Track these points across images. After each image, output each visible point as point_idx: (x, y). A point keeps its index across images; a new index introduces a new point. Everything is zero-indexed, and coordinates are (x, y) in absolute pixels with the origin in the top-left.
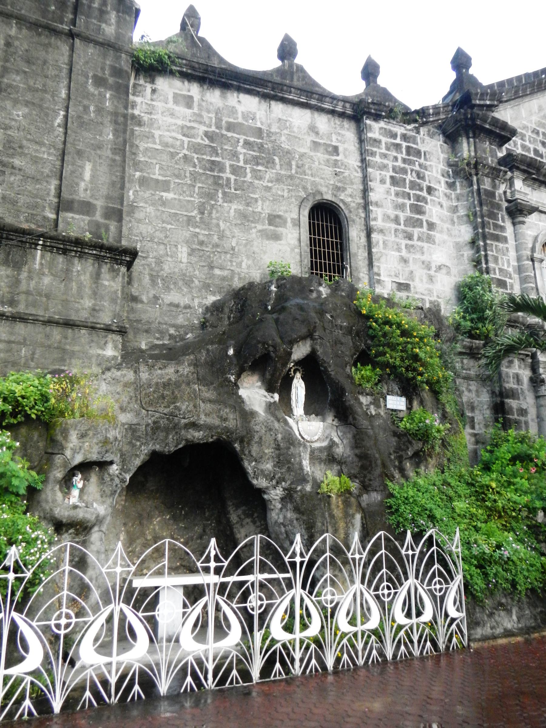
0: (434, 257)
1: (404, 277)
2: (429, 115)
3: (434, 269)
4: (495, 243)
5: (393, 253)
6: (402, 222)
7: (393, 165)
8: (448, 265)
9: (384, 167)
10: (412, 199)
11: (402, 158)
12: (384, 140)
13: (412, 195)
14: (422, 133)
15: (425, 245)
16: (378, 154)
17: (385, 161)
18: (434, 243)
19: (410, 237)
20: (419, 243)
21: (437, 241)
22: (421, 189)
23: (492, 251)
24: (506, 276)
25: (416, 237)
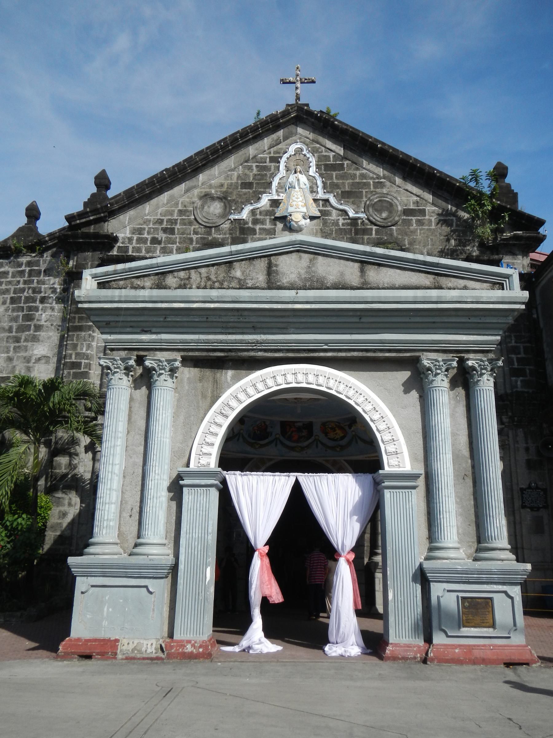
0: (36, 352)
1: (7, 371)
2: (47, 241)
3: (33, 361)
4: (75, 334)
5: (3, 355)
6: (14, 330)
7: (15, 288)
8: (49, 355)
9: (7, 291)
10: (25, 311)
11: (24, 280)
12: (11, 270)
13: (25, 308)
14: (45, 256)
15: (29, 344)
16: (4, 283)
17: (8, 287)
18: (38, 340)
19: (17, 340)
20: (25, 344)
21: (41, 338)
22: (34, 301)
23: (73, 340)
24: (83, 358)
25: (22, 340)
